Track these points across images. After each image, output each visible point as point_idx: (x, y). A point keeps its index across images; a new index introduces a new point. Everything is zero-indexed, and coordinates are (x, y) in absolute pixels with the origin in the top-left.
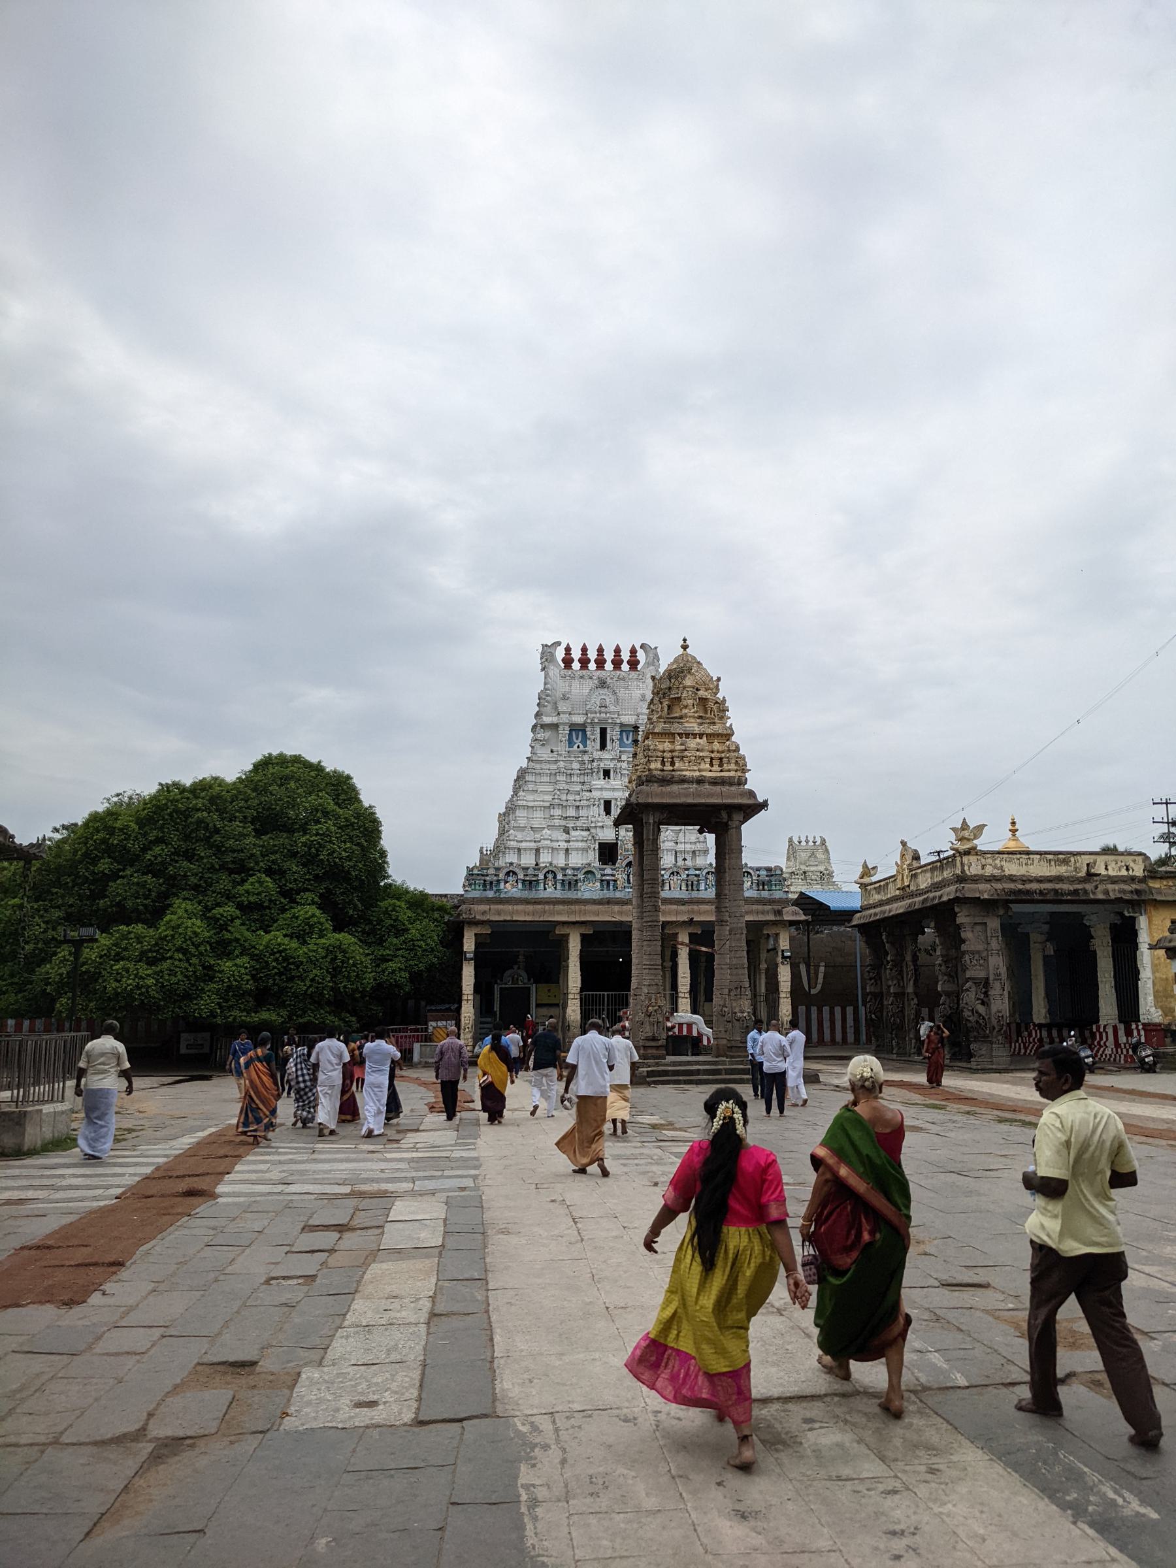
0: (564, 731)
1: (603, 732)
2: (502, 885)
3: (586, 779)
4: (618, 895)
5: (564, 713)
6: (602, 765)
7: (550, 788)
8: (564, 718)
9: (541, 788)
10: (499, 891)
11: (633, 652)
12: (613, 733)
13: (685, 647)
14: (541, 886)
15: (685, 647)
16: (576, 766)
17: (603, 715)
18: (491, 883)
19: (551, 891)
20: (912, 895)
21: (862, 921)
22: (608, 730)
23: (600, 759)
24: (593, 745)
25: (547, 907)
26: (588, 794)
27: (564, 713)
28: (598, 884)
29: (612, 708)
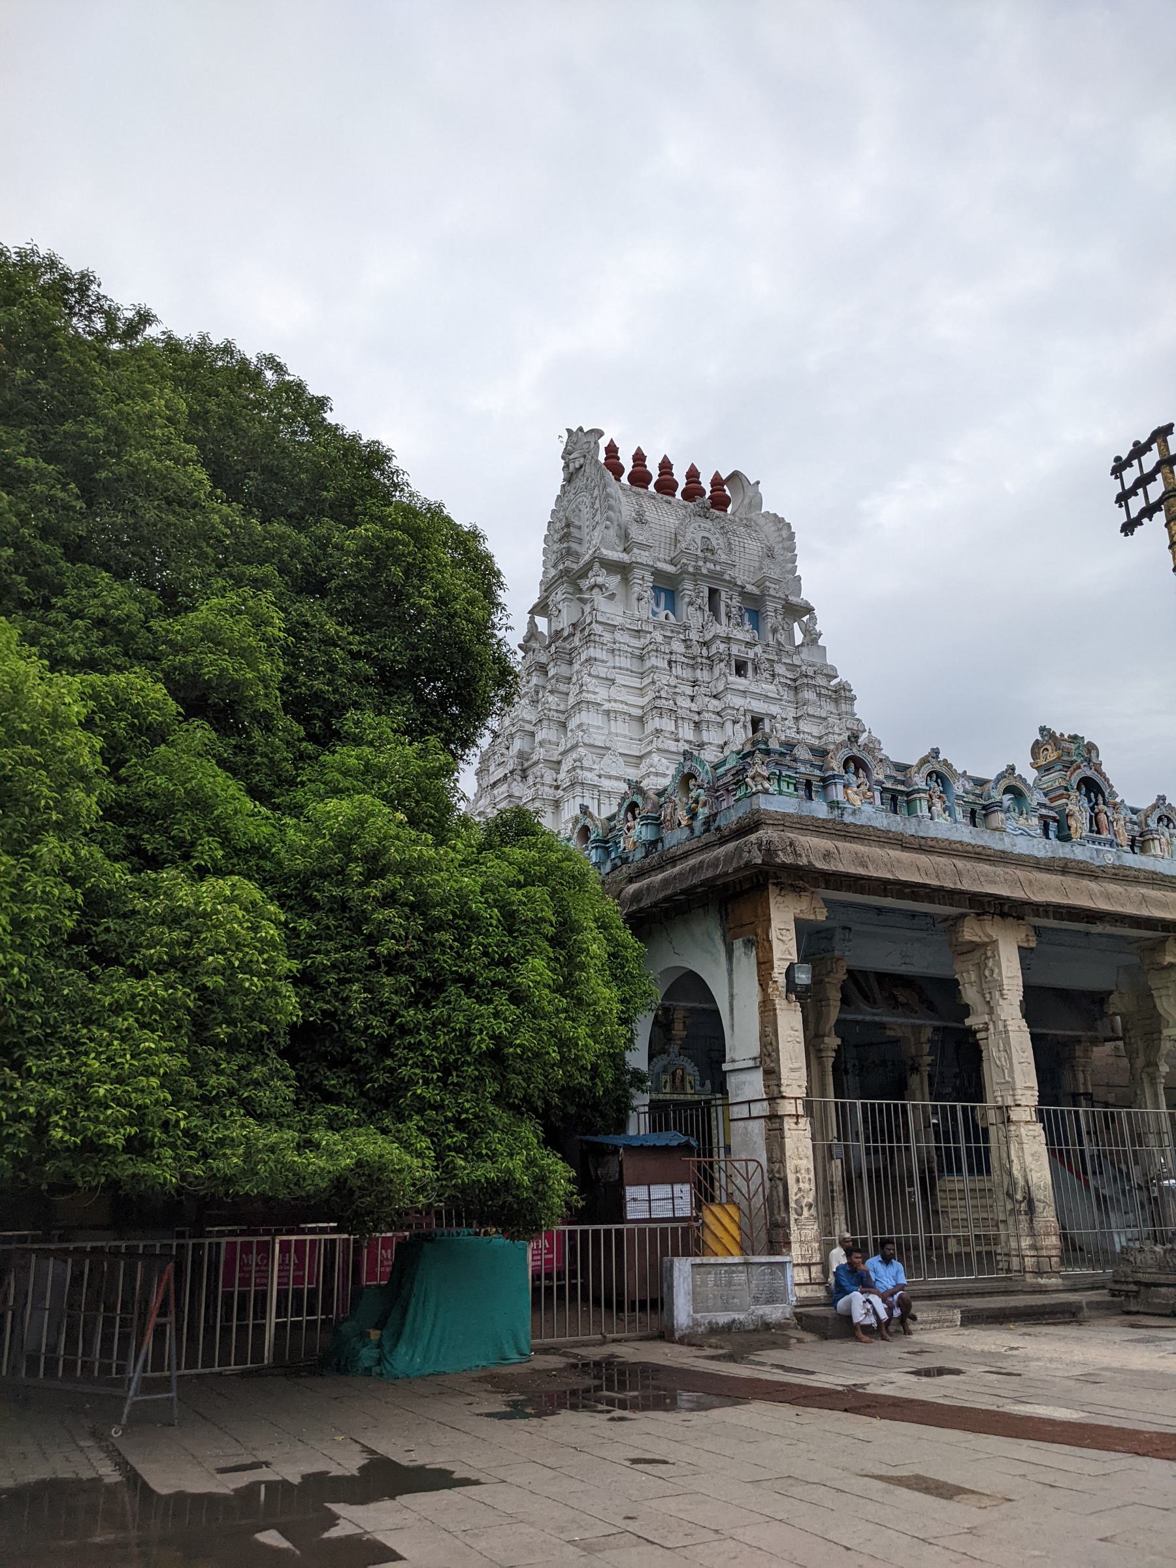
0: (642, 583)
1: (713, 593)
2: (837, 792)
3: (703, 675)
4: (1080, 853)
6: (735, 649)
7: (636, 682)
8: (643, 557)
9: (620, 679)
10: (833, 805)
11: (717, 482)
12: (729, 600)
14: (922, 809)
16: (678, 647)
17: (710, 566)
18: (808, 784)
22: (723, 595)
23: (728, 640)
24: (694, 617)
25: (960, 863)
26: (715, 702)
28: (1035, 821)
29: (724, 558)
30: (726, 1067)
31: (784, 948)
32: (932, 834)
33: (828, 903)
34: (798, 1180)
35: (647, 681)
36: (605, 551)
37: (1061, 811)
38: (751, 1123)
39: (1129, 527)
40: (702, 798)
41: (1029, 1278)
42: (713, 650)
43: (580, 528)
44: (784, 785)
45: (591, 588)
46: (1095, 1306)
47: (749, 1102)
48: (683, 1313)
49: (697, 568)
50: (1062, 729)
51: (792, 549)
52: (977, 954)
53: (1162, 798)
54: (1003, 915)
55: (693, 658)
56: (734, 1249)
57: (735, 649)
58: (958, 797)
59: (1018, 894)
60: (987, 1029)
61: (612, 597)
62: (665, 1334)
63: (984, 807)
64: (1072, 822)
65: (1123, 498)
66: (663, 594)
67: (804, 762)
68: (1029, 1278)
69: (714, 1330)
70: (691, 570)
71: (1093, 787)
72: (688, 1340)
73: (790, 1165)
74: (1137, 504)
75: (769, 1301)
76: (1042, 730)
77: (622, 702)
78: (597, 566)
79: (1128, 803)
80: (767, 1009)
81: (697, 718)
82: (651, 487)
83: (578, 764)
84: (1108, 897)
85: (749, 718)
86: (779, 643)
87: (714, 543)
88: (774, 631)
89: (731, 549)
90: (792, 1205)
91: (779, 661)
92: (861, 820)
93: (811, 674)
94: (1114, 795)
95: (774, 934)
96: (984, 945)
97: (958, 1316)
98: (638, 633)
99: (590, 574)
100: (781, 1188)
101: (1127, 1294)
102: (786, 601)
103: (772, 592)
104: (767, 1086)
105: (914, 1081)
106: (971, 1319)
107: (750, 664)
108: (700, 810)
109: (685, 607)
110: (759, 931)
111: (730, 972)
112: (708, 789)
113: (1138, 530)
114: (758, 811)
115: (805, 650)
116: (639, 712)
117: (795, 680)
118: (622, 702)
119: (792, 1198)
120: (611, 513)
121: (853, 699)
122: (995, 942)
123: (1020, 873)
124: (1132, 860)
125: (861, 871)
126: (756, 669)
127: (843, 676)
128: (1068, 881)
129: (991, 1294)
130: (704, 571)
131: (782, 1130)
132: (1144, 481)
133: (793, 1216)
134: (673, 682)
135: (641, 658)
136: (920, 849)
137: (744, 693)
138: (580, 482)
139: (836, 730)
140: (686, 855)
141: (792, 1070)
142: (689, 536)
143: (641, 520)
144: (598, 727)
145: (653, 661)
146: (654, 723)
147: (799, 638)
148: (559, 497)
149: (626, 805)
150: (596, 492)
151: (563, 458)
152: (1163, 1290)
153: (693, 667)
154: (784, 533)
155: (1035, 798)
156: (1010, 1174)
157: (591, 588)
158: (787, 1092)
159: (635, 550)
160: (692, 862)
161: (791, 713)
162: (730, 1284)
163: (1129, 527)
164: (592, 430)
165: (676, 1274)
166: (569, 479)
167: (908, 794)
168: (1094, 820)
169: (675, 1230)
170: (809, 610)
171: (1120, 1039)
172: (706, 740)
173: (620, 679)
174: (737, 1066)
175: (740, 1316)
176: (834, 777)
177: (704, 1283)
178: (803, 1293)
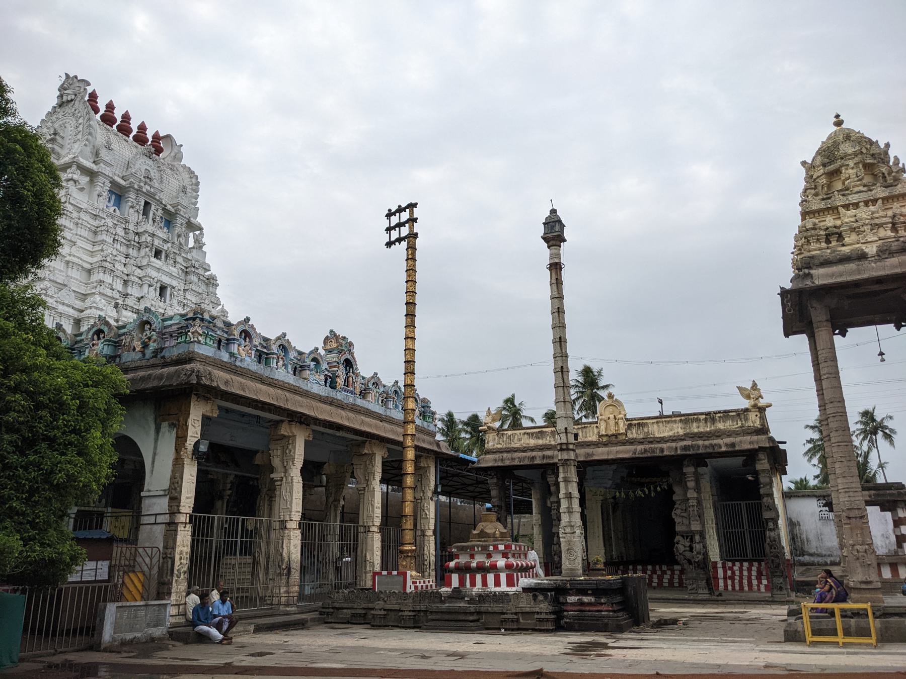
0: (102, 186)
2: (234, 348)
3: (133, 252)
4: (339, 396)
5: (106, 163)
6: (156, 242)
7: (89, 247)
8: (107, 170)
9: (80, 243)
10: (232, 355)
11: (156, 137)
13: (839, 123)
15: (839, 123)
16: (120, 231)
18: (220, 341)
19: (283, 374)
20: (632, 442)
21: (507, 463)
22: (153, 207)
24: (134, 216)
26: (139, 271)
27: (106, 163)
28: (323, 377)
29: (157, 185)
30: (142, 494)
31: (194, 431)
32: (276, 377)
33: (220, 408)
34: (181, 559)
35: (97, 248)
36: (81, 160)
37: (334, 374)
38: (155, 526)
39: (389, 244)
40: (154, 337)
41: (282, 608)
42: (143, 239)
43: (63, 138)
44: (208, 340)
45: (68, 180)
46: (313, 620)
47: (156, 515)
48: (107, 634)
49: (141, 187)
50: (340, 333)
51: (197, 191)
52: (283, 441)
53: (376, 374)
54: (301, 423)
55: (129, 241)
56: (138, 597)
57: (156, 242)
58: (291, 360)
59: (312, 413)
60: (282, 480)
61: (82, 189)
62: (95, 647)
63: (301, 367)
64: (338, 380)
65: (389, 229)
66: (113, 196)
67: (219, 328)
68: (282, 608)
69: (124, 643)
70: (136, 187)
71: (349, 364)
72: (109, 650)
73: (178, 550)
74: (395, 235)
75: (155, 626)
76: (331, 331)
77: (78, 258)
78: (74, 167)
79: (362, 374)
80: (178, 464)
81: (126, 278)
82: (115, 126)
83: (43, 291)
84: (348, 419)
85: (159, 285)
86: (180, 244)
87: (152, 174)
88: (179, 236)
89: (162, 181)
90: (176, 572)
91: (180, 255)
92: (244, 365)
93: (197, 266)
94: (357, 369)
95: (190, 422)
96: (289, 437)
97: (252, 628)
98: (96, 217)
99: (69, 171)
100: (170, 563)
101: (328, 614)
102: (189, 220)
103: (182, 213)
104: (170, 506)
105: (219, 504)
106: (259, 629)
107: (163, 253)
108: (151, 344)
109: (127, 208)
110: (181, 419)
111: (156, 440)
112: (158, 333)
113: (393, 246)
114: (193, 352)
115: (194, 251)
116: (89, 267)
117: (187, 268)
118: (78, 258)
119: (176, 568)
120: (90, 137)
121: (217, 285)
122: (295, 436)
123: (314, 403)
124: (360, 402)
125: (242, 393)
126: (167, 257)
127: (214, 271)
128: (333, 409)
129: (265, 616)
130: (144, 190)
131: (176, 531)
132: (400, 225)
133: (175, 578)
134: (115, 253)
135: (95, 233)
136: (270, 385)
137: (159, 270)
138: (68, 109)
139: (207, 302)
140: (136, 369)
141: (187, 498)
142: (137, 166)
143: (108, 147)
144: (60, 271)
145: (104, 237)
146: (98, 276)
147: (191, 244)
148: (49, 113)
149: (94, 330)
150: (81, 121)
151: (59, 90)
152: (345, 611)
153: (127, 246)
154: (194, 181)
155: (324, 366)
156: (282, 555)
157: (68, 180)
158: (182, 510)
159: (102, 165)
160: (141, 373)
161: (182, 287)
162: (136, 617)
163: (389, 244)
164: (83, 80)
165: (107, 612)
166: (61, 105)
167: (267, 354)
168: (347, 380)
169: (81, 588)
170: (201, 229)
171: (322, 486)
172: (129, 292)
173: (80, 243)
174: (151, 494)
175: (139, 635)
176: (234, 339)
177: (121, 617)
178: (173, 620)
